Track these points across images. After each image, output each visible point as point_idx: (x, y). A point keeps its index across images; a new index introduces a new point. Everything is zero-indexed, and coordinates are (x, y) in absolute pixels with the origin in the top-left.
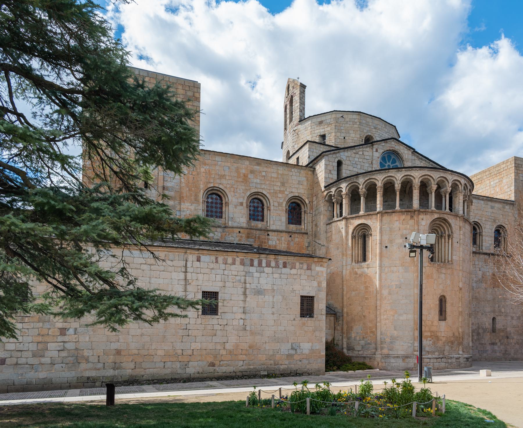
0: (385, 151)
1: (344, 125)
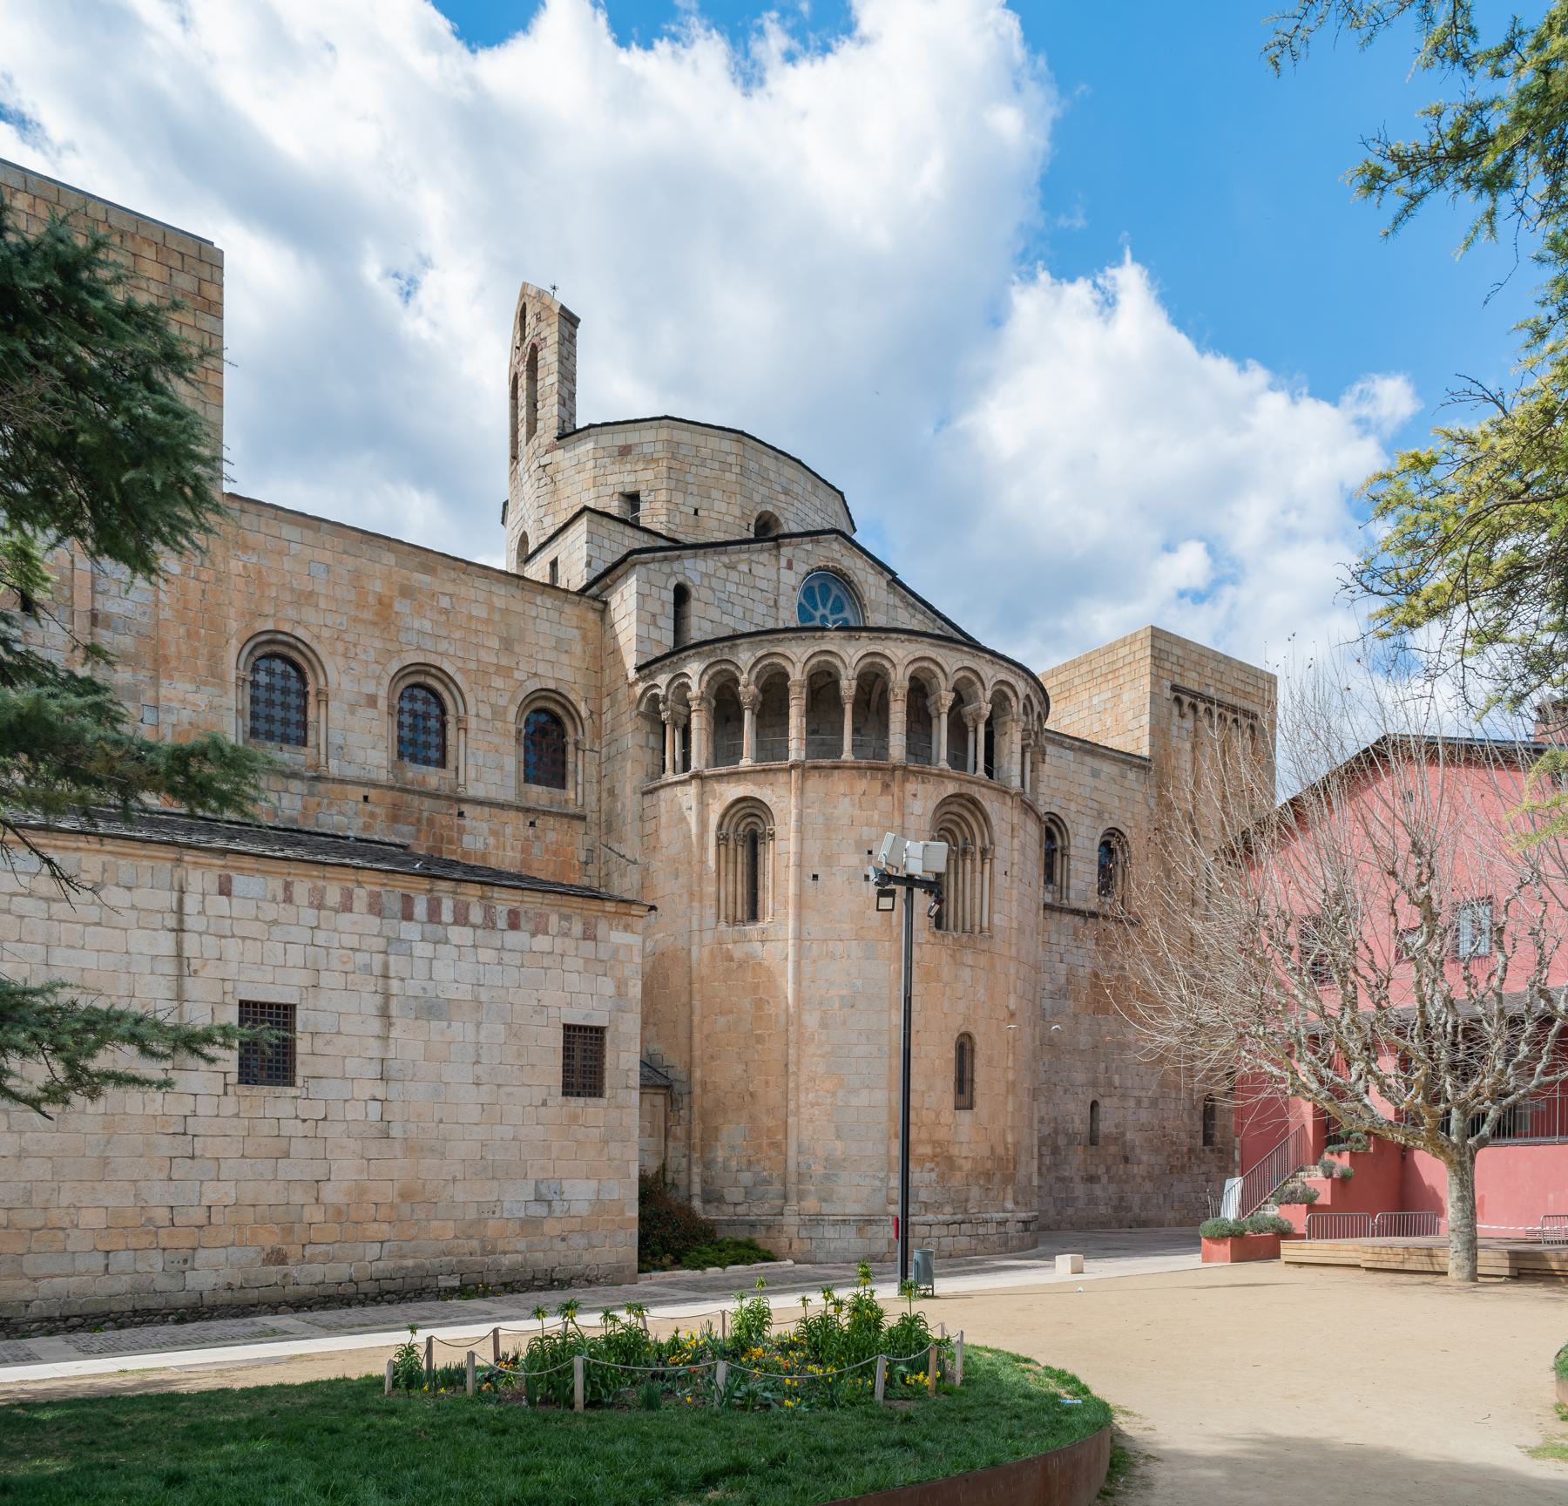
0: (813, 571)
1: (693, 469)
